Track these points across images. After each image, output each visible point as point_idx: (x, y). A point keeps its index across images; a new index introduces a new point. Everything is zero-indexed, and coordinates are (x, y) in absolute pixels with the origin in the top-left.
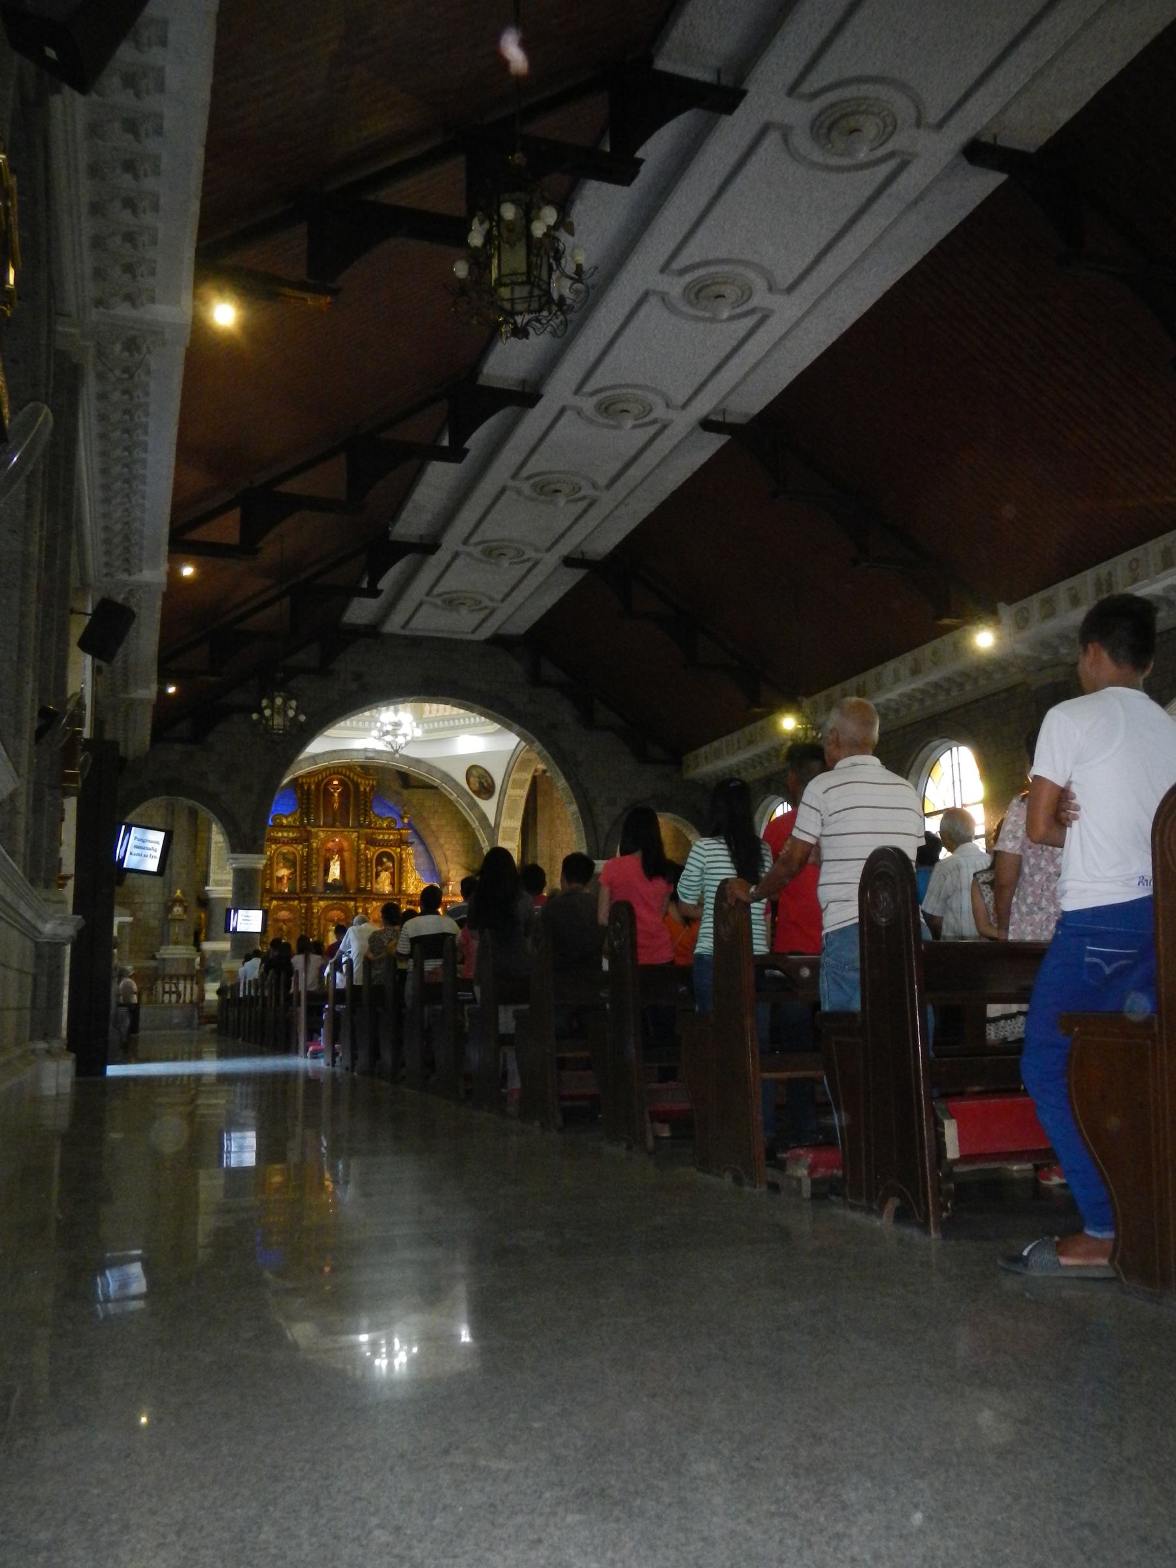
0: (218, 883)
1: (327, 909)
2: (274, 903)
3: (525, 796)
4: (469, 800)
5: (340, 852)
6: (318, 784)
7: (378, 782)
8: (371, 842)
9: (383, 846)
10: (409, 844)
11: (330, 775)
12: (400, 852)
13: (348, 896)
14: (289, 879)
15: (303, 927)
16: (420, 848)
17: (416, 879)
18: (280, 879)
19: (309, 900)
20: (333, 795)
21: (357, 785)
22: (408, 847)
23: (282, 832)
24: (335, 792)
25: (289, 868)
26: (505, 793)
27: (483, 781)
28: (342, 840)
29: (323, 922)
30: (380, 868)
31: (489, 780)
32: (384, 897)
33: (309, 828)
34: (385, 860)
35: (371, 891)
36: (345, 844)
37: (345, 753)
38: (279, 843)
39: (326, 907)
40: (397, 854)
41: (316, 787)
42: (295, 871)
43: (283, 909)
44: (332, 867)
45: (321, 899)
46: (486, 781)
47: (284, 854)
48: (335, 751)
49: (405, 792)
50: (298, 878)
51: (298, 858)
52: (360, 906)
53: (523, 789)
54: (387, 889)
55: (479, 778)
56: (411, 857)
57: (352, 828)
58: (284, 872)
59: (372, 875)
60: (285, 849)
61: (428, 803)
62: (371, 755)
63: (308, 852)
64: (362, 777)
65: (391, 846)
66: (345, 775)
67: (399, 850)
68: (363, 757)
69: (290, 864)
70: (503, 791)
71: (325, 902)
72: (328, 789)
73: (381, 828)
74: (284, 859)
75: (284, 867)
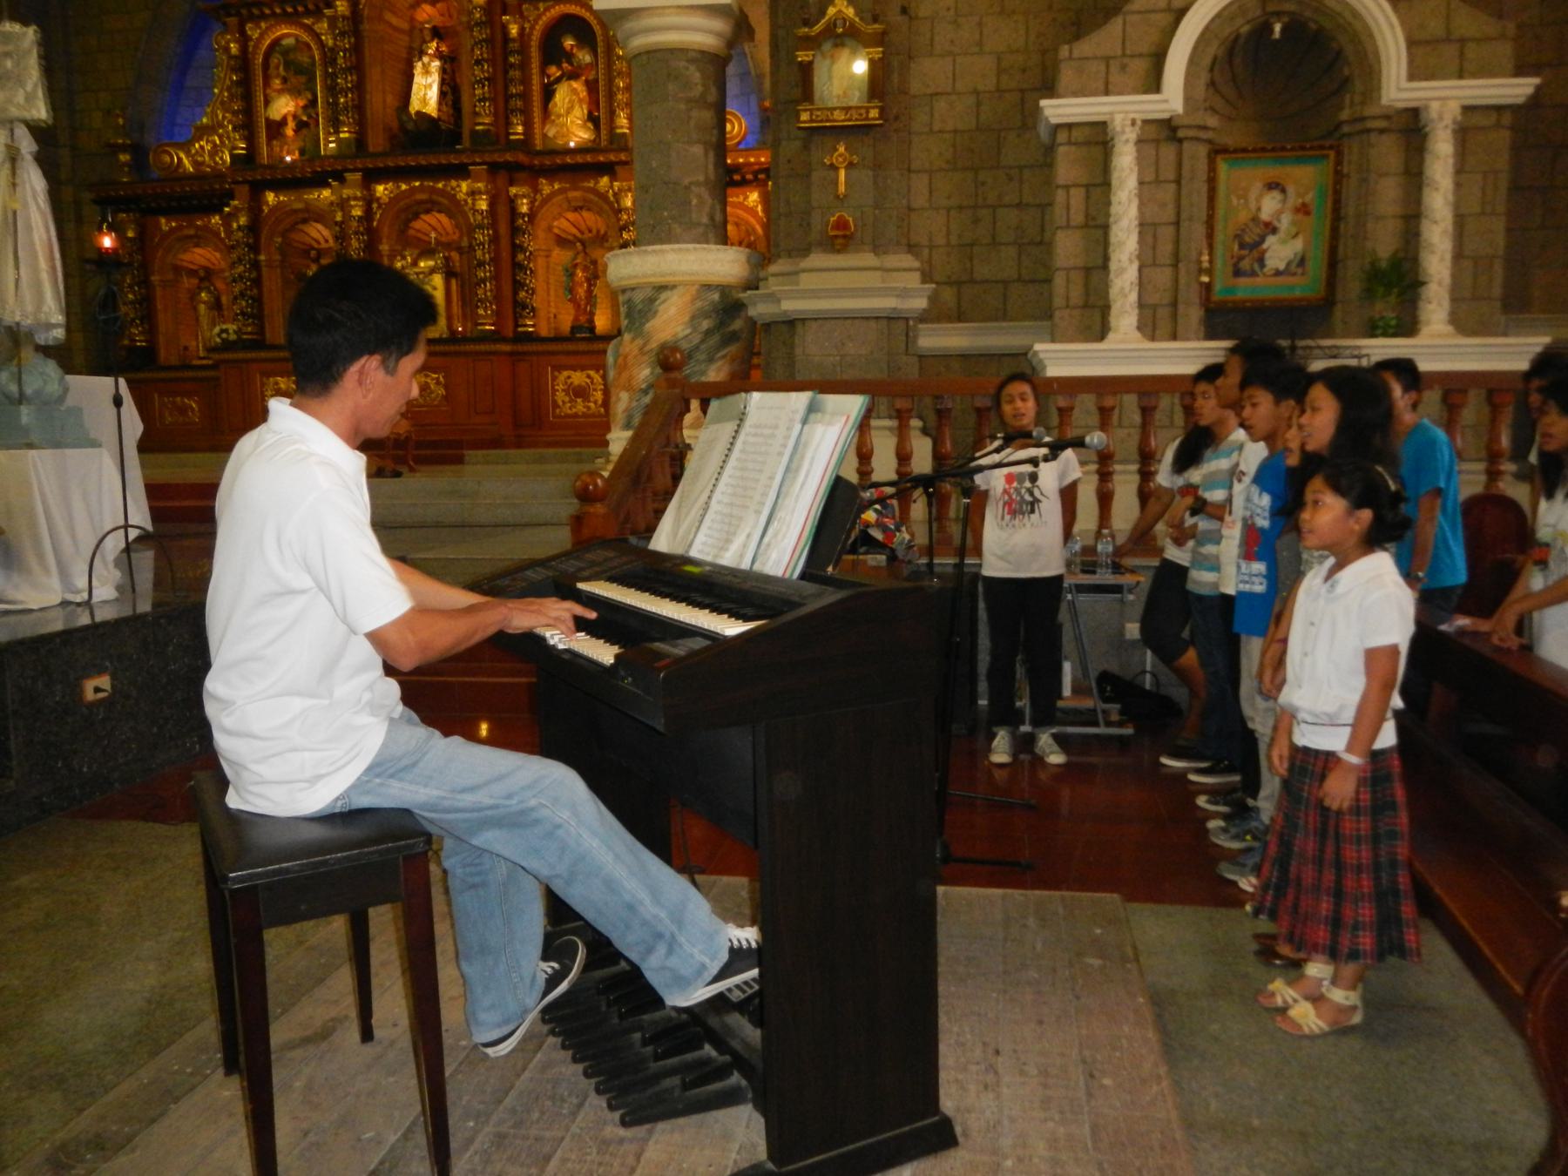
1: (409, 211)
2: (271, 197)
14: (301, 126)
18: (276, 128)
25: (295, 92)
30: (554, 71)
34: (569, 42)
35: (526, 144)
38: (263, 17)
39: (394, 200)
42: (313, 103)
44: (419, 79)
45: (372, 176)
47: (286, 52)
58: (284, 106)
69: (303, 79)
71: (390, 185)
74: (287, 68)
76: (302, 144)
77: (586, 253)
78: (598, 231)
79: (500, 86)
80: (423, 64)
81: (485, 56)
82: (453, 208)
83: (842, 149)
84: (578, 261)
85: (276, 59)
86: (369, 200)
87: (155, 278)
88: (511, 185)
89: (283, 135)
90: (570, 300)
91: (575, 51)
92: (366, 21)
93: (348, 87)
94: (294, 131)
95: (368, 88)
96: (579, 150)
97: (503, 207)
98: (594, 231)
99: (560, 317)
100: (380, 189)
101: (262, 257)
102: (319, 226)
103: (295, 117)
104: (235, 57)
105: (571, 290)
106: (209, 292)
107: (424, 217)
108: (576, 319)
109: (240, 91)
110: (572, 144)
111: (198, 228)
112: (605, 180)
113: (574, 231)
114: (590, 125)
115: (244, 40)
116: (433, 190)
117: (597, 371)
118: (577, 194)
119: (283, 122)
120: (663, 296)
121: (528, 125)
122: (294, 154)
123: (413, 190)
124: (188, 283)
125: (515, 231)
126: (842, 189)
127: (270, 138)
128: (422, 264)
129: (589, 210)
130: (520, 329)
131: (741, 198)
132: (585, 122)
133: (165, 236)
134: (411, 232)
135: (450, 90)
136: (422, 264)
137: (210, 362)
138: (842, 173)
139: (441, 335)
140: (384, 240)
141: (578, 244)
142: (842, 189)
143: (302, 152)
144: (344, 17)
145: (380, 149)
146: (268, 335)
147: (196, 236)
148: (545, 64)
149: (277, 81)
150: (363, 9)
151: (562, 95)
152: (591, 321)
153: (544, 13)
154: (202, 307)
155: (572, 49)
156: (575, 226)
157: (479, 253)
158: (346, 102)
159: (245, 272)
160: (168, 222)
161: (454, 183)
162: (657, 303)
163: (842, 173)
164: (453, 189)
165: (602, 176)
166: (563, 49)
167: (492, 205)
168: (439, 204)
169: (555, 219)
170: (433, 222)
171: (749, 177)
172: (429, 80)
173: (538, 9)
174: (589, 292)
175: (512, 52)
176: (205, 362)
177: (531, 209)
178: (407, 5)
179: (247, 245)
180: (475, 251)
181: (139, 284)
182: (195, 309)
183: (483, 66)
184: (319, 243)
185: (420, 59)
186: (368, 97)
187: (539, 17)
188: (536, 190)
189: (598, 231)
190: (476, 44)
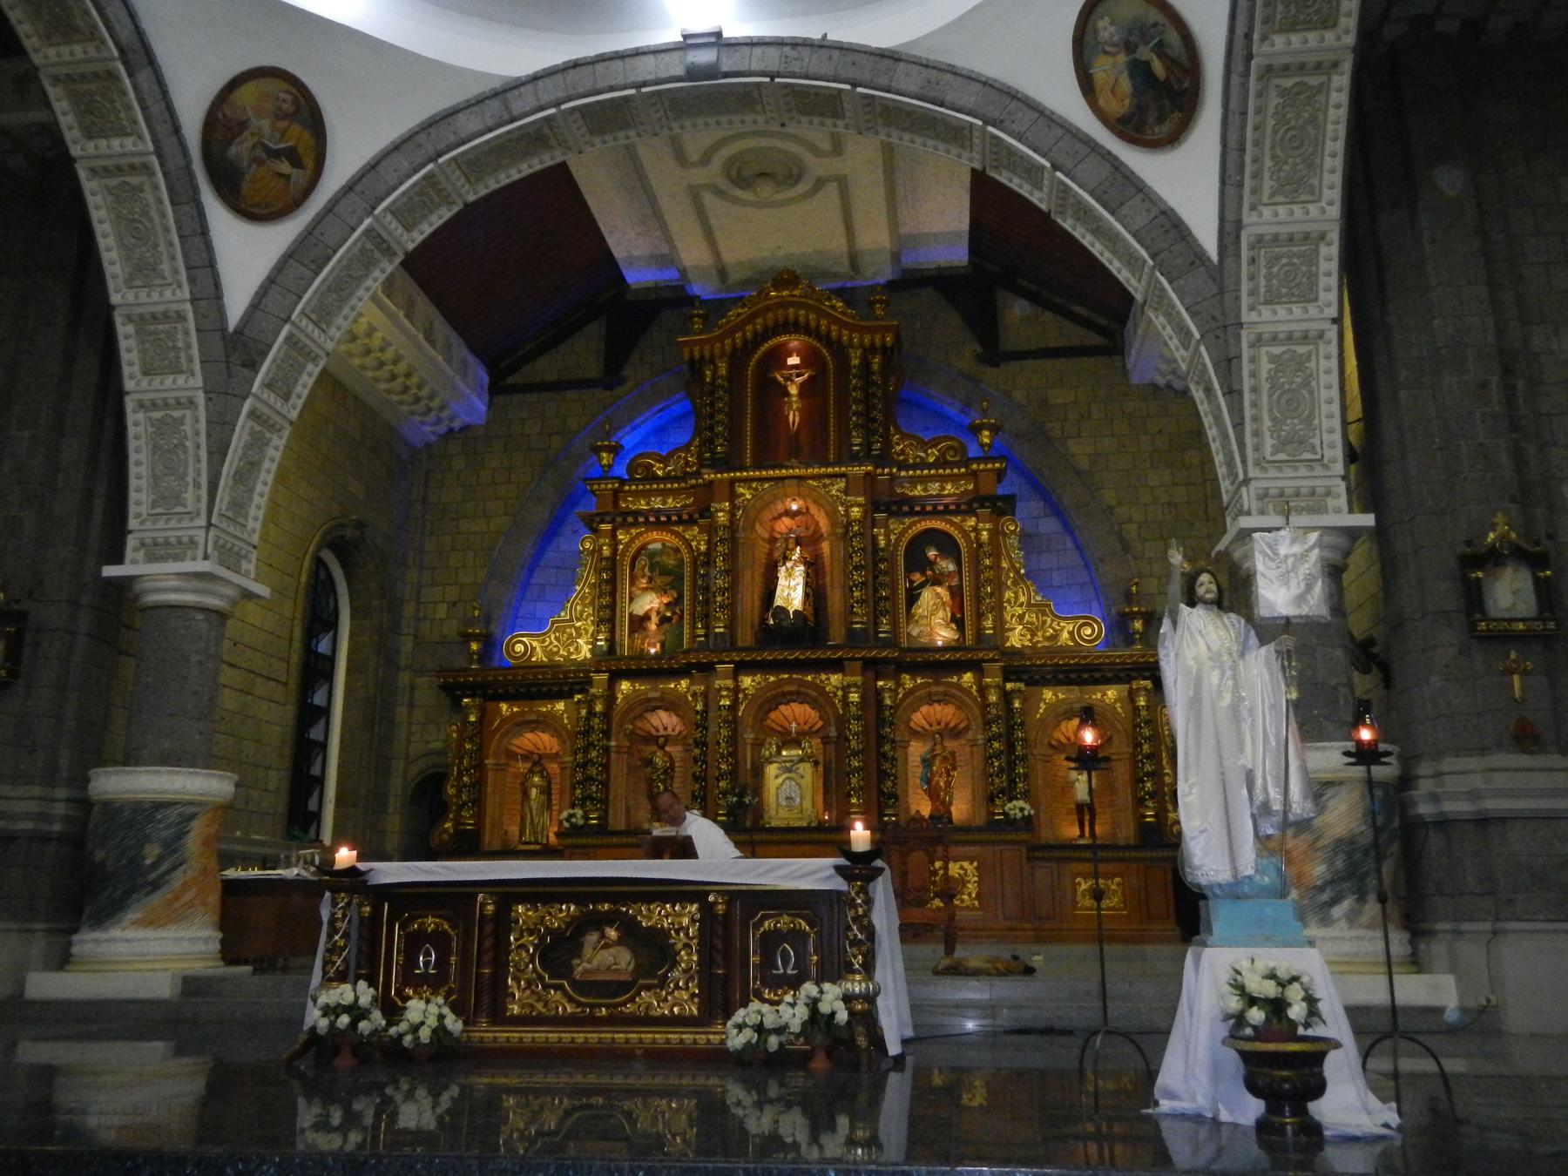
0: (157, 551)
1: (771, 701)
2: (625, 686)
3: (1347, 66)
4: (1105, 170)
5: (809, 541)
6: (737, 359)
7: (897, 338)
8: (887, 503)
9: (924, 514)
10: (1002, 506)
11: (768, 334)
12: (975, 529)
13: (820, 654)
14: (663, 620)
15: (697, 751)
16: (1050, 525)
17: (1029, 605)
18: (639, 623)
19: (707, 669)
20: (788, 394)
21: (840, 351)
22: (1002, 513)
23: (647, 494)
24: (789, 379)
25: (662, 591)
26: (1249, 57)
27: (1144, 53)
28: (813, 509)
29: (750, 736)
30: (917, 578)
31: (1173, 37)
32: (931, 657)
33: (709, 476)
34: (932, 553)
35: (892, 643)
36: (824, 523)
37: (619, 63)
38: (635, 524)
40: (966, 535)
41: (730, 369)
43: (652, 705)
44: (782, 582)
45: (741, 668)
46: (1160, 49)
47: (652, 555)
48: (575, 65)
49: (990, 373)
50: (686, 617)
51: (687, 559)
52: (855, 685)
53: (1328, 22)
54: (943, 635)
55: (1129, 48)
56: (1014, 541)
57: (827, 465)
58: (649, 602)
59: (894, 592)
60: (656, 540)
61: (1058, 396)
62: (705, 57)
63: (709, 542)
64: (852, 328)
65: (947, 511)
66: (819, 337)
67: (972, 522)
68: (679, 71)
69: (668, 579)
70: (1239, 49)
71: (758, 678)
72: (775, 378)
73: (923, 465)
74: (651, 569)
75: (652, 587)
76: (663, 637)
79: (871, 591)
82: (820, 699)
83: (1513, 655)
85: (643, 561)
86: (737, 690)
87: (489, 762)
89: (645, 629)
96: (944, 649)
97: (872, 699)
98: (943, 725)
100: (747, 681)
101: (613, 743)
102: (663, 714)
103: (658, 613)
104: (608, 558)
105: (929, 782)
106: (542, 777)
108: (934, 809)
109: (609, 588)
110: (940, 643)
111: (540, 714)
112: (968, 677)
113: (924, 723)
114: (954, 626)
115: (615, 542)
116: (802, 683)
117: (971, 863)
118: (941, 689)
119: (647, 617)
120: (1330, 792)
121: (895, 625)
122: (655, 646)
123: (780, 682)
124: (523, 767)
125: (881, 722)
126: (1518, 693)
127: (631, 632)
128: (784, 753)
131: (1099, 696)
133: (504, 721)
134: (769, 722)
135: (815, 591)
136: (784, 753)
137: (538, 847)
138: (1516, 679)
139: (809, 823)
142: (1518, 693)
143: (663, 646)
144: (724, 527)
145: (748, 644)
146: (611, 821)
147: (537, 722)
148: (909, 570)
149: (644, 581)
151: (927, 596)
152: (950, 813)
153: (910, 527)
154: (534, 792)
157: (853, 744)
160: (510, 707)
161: (823, 677)
162: (1325, 798)
163: (1516, 679)
164: (822, 681)
166: (927, 558)
167: (862, 697)
168: (807, 695)
171: (1110, 675)
172: (793, 583)
173: (903, 523)
174: (948, 783)
175: (883, 560)
176: (532, 847)
177: (894, 702)
179: (602, 732)
180: (849, 741)
181: (475, 767)
182: (526, 794)
184: (658, 731)
185: (784, 564)
186: (739, 596)
187: (905, 530)
188: (899, 684)
189: (947, 725)
190: (854, 552)
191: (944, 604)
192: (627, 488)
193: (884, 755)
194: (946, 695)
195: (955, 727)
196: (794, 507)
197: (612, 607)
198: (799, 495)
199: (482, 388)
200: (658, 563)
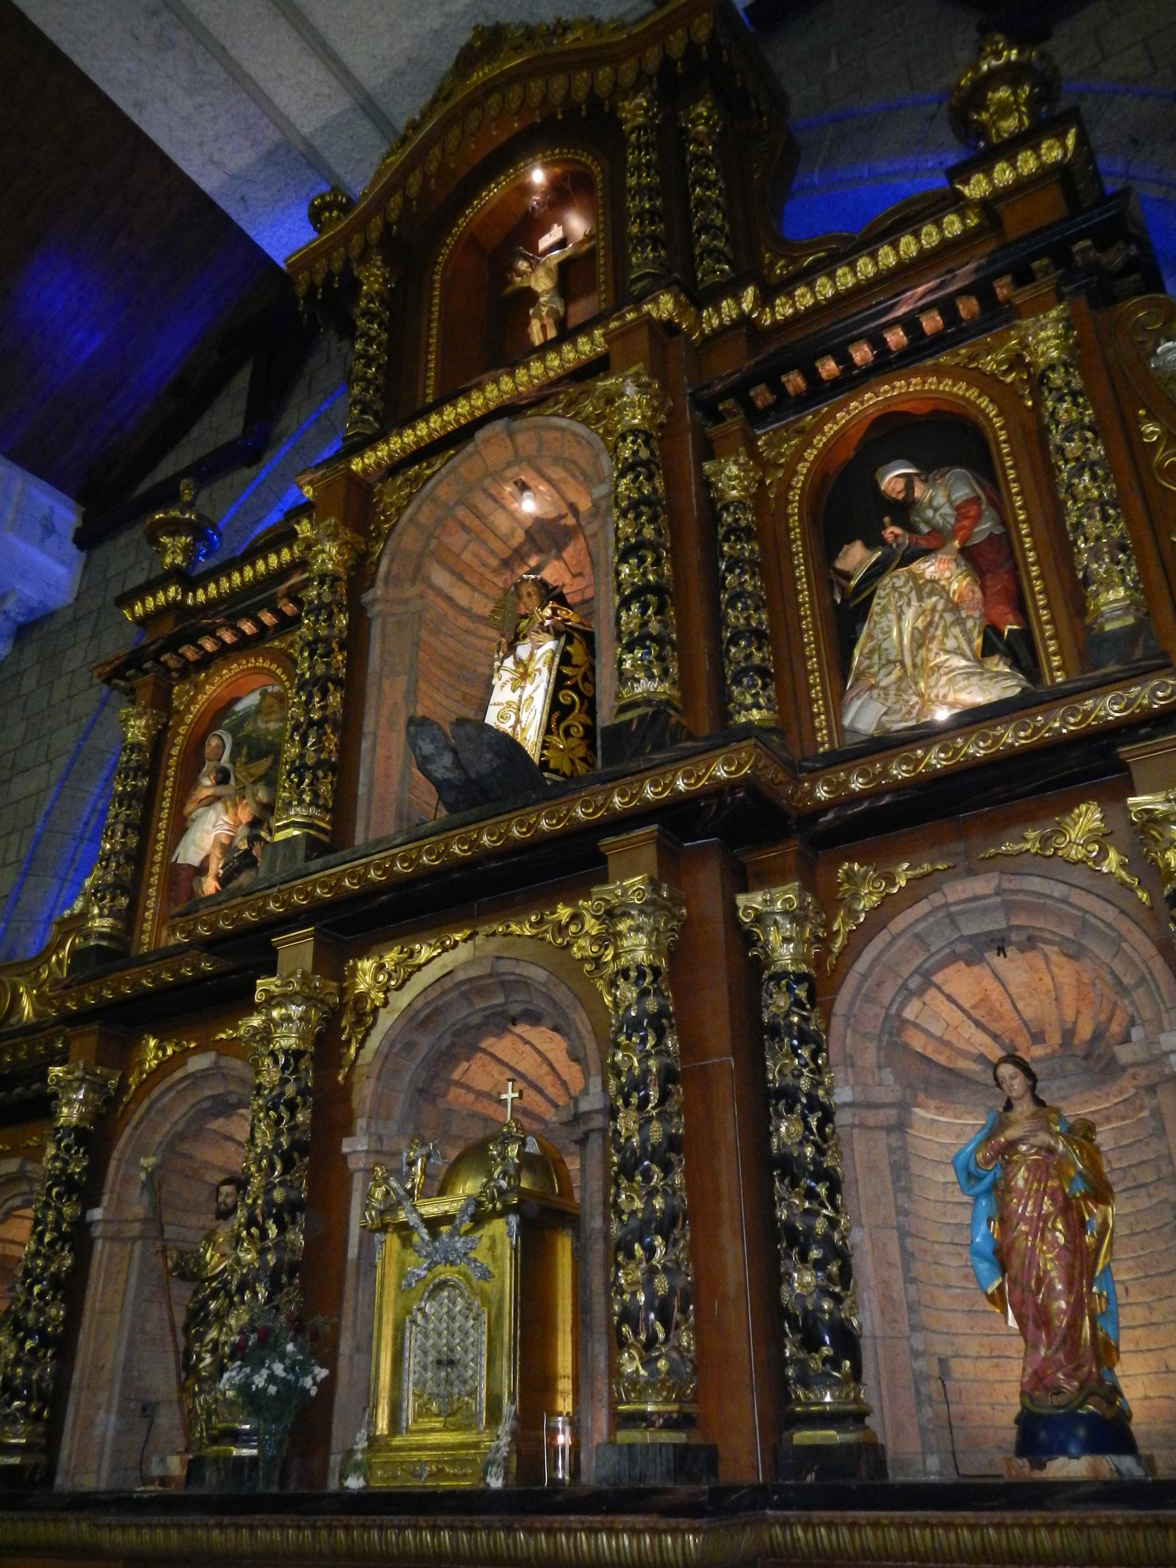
40: (988, 383)
77: (1040, 1103)
78: (1068, 1035)
79: (698, 611)
80: (518, 662)
81: (649, 532)
84: (1012, 1133)
88: (745, 890)
90: (999, 1299)
91: (919, 491)
92: (379, 583)
93: (311, 723)
94: (218, 878)
95: (369, 724)
98: (1054, 1039)
99: (958, 1367)
101: (97, 1214)
104: (135, 747)
107: (502, 1046)
113: (981, 1042)
114: (998, 665)
118: (982, 885)
129: (1031, 943)
130: (803, 1437)
132: (981, 664)
140: (361, 1123)
141: (1006, 1070)
150: (377, 564)
155: (909, 487)
156: (978, 1024)
158: (301, 756)
159: (37, 1254)
161: (564, 912)
164: (561, 929)
165: (1068, 807)
169: (908, 994)
170: (528, 1063)
178: (494, 562)
183: (642, 560)
185: (512, 648)
186: (365, 745)
189: (1068, 1035)
191: (954, 607)
192: (201, 596)
193: (789, 1166)
194: (1009, 908)
195: (1098, 1035)
196: (529, 506)
197: (138, 858)
198: (517, 459)
199: (49, 529)
200: (248, 737)
